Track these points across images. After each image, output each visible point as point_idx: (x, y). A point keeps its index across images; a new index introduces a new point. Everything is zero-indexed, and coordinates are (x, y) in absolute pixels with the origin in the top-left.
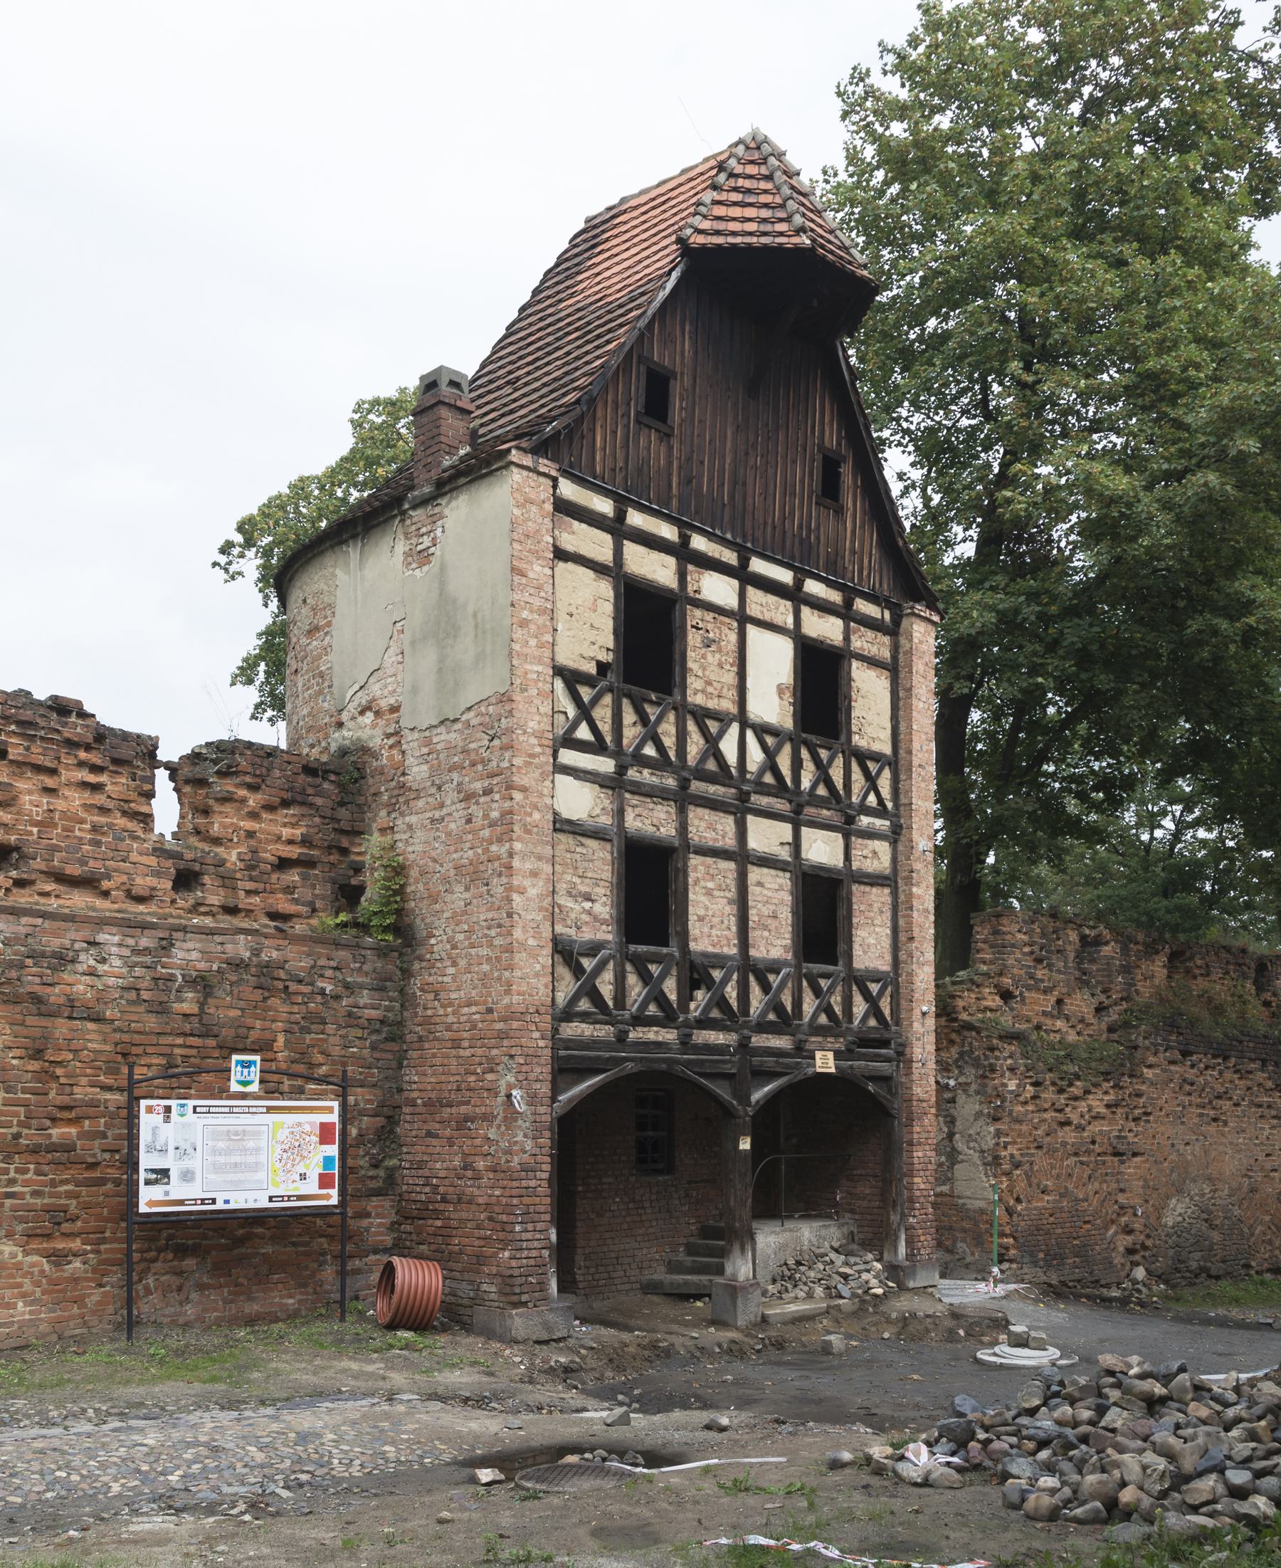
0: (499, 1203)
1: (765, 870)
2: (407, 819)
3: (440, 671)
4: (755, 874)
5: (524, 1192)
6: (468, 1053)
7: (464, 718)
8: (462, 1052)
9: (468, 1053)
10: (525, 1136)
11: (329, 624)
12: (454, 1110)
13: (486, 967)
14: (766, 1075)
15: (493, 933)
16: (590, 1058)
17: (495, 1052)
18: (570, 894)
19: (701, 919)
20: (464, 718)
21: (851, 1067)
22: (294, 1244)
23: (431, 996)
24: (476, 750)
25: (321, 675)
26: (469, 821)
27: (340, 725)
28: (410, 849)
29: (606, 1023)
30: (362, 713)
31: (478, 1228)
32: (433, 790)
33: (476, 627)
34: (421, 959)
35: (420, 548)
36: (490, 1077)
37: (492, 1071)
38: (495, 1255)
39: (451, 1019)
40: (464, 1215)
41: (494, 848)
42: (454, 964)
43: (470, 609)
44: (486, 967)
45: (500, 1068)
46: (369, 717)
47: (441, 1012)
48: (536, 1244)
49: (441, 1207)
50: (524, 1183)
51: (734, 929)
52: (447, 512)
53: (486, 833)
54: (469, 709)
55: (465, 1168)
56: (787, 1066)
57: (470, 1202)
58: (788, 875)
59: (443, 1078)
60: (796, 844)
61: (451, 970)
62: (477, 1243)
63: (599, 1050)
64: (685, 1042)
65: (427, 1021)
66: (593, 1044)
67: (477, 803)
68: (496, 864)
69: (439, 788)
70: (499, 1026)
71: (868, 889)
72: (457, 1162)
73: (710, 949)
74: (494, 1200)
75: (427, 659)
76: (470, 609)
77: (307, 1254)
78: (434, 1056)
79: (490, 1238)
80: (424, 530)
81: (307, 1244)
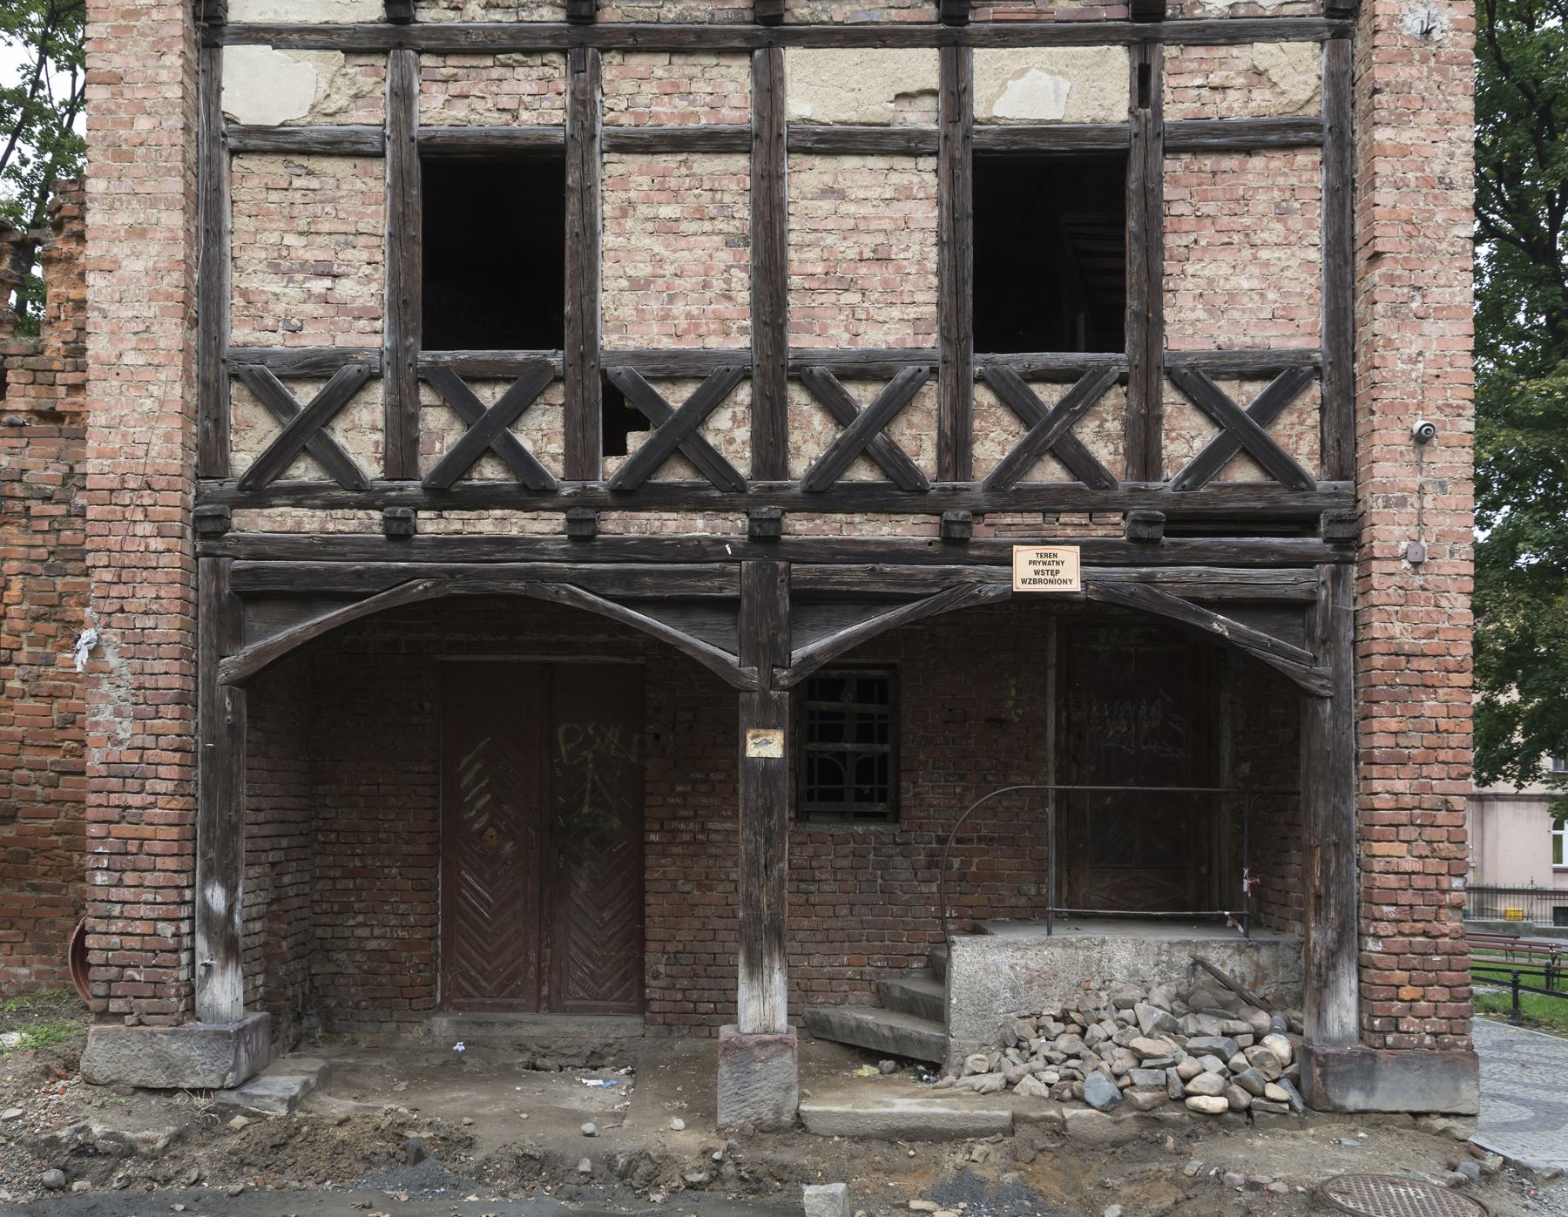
1: (851, 162)
4: (806, 178)
5: (114, 814)
10: (118, 713)
14: (816, 602)
16: (311, 572)
18: (275, 268)
19: (637, 285)
21: (1147, 580)
22: (35, 888)
29: (362, 506)
48: (144, 911)
50: (115, 799)
51: (744, 297)
56: (908, 580)
58: (931, 163)
60: (955, 90)
63: (343, 556)
64: (582, 537)
66: (328, 545)
71: (1230, 162)
73: (667, 344)
77: (54, 904)
81: (58, 889)
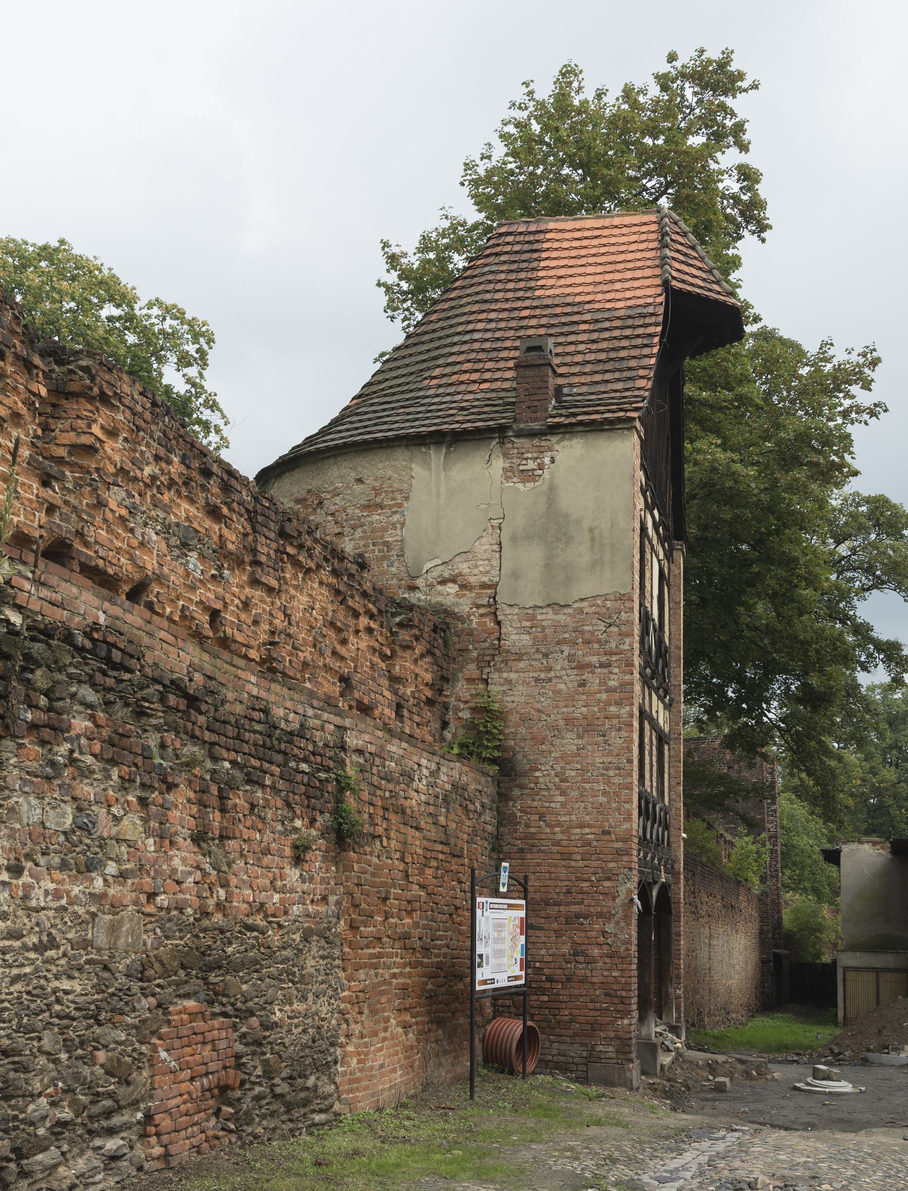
0: (617, 982)
2: (505, 675)
3: (547, 565)
6: (580, 864)
7: (576, 605)
8: (573, 863)
9: (580, 864)
11: (400, 505)
12: (562, 908)
13: (602, 799)
15: (611, 773)
17: (611, 865)
20: (576, 605)
23: (537, 817)
24: (592, 633)
25: (387, 544)
26: (583, 684)
27: (413, 588)
28: (508, 699)
30: (443, 582)
31: (592, 1001)
32: (539, 656)
33: (593, 539)
34: (522, 787)
35: (522, 468)
36: (607, 884)
37: (609, 879)
38: (612, 1023)
39: (559, 837)
40: (576, 992)
41: (613, 709)
42: (563, 793)
43: (586, 524)
44: (602, 799)
45: (620, 878)
46: (452, 588)
47: (548, 830)
49: (548, 985)
52: (557, 447)
53: (604, 696)
54: (582, 600)
55: (575, 954)
57: (582, 981)
59: (549, 883)
61: (562, 799)
62: (592, 1013)
65: (532, 836)
67: (593, 672)
68: (615, 721)
69: (546, 655)
70: (620, 845)
72: (566, 949)
74: (610, 979)
75: (532, 557)
76: (586, 524)
78: (538, 865)
79: (606, 1009)
80: (529, 455)
